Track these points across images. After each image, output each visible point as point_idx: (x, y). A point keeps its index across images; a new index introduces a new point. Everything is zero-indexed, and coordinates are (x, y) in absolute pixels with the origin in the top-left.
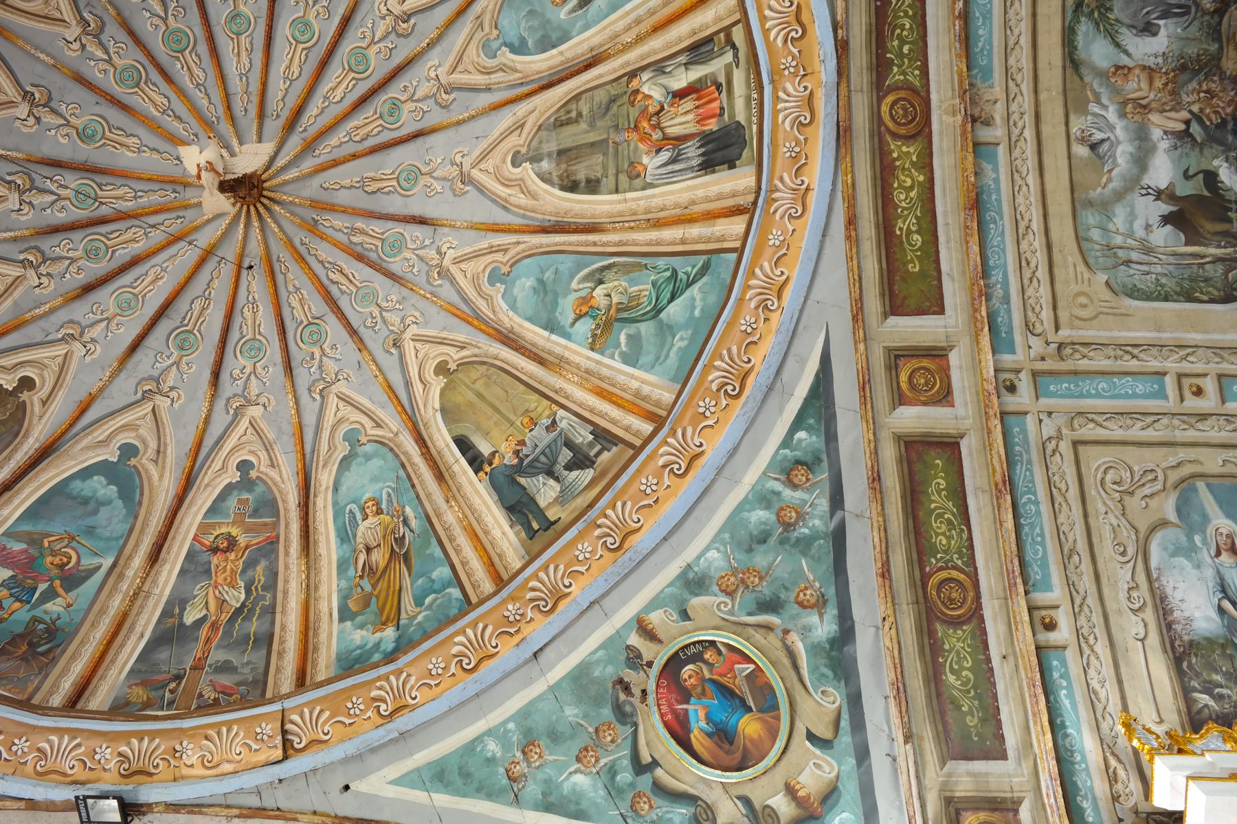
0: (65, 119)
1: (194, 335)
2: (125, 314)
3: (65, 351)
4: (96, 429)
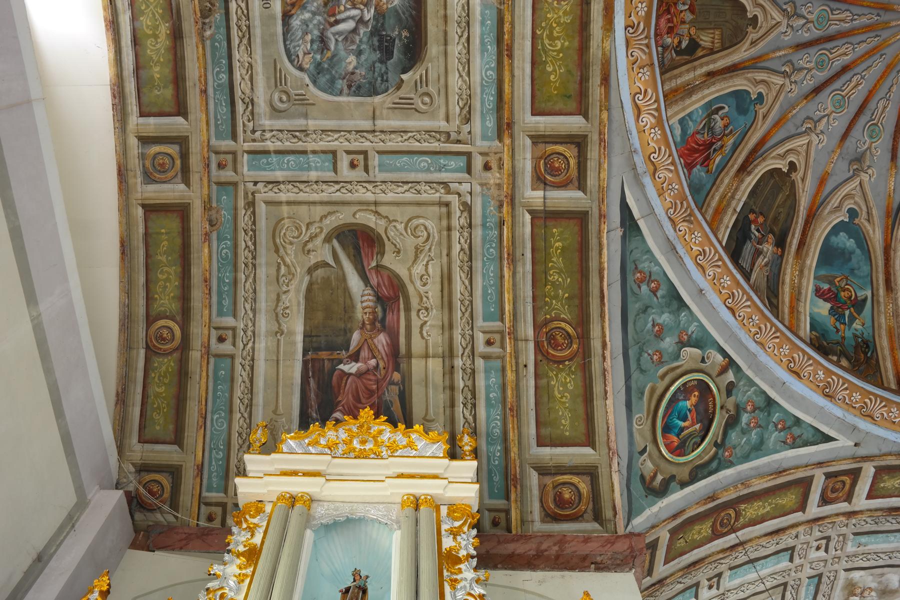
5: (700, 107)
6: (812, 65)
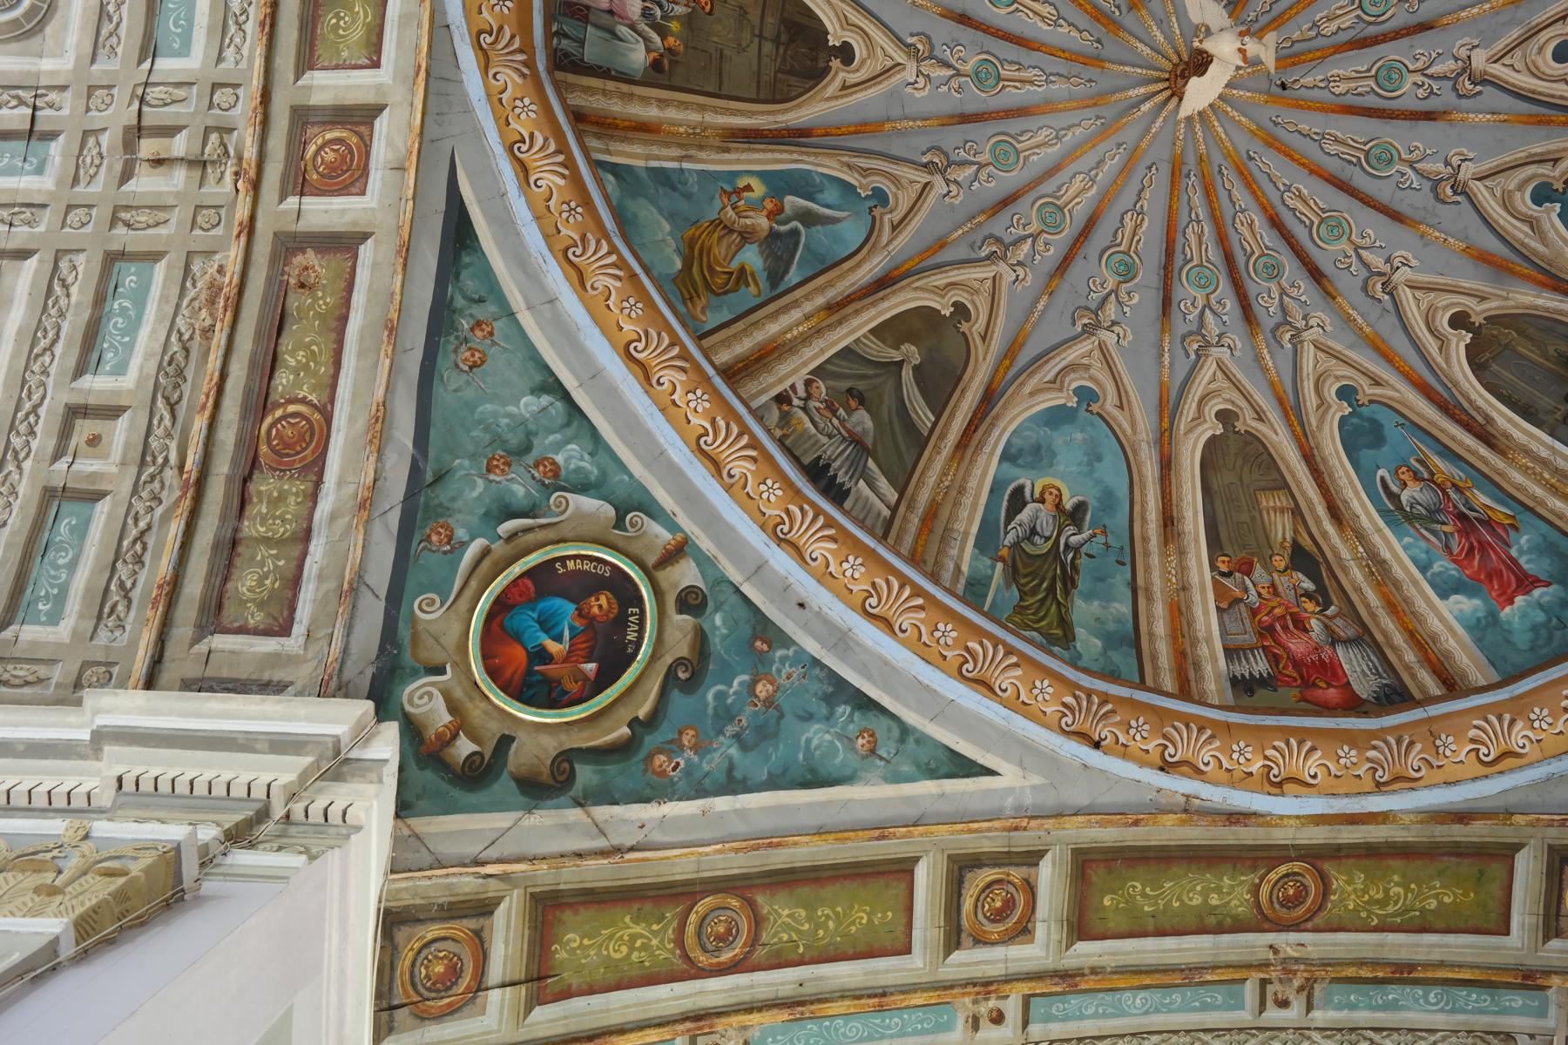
0: (1109, 294)
1: (1371, 148)
2: (1347, 230)
3: (1407, 289)
4: (1514, 237)
5: (1400, 541)
6: (1273, 286)
